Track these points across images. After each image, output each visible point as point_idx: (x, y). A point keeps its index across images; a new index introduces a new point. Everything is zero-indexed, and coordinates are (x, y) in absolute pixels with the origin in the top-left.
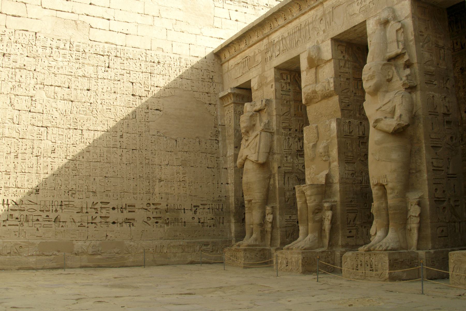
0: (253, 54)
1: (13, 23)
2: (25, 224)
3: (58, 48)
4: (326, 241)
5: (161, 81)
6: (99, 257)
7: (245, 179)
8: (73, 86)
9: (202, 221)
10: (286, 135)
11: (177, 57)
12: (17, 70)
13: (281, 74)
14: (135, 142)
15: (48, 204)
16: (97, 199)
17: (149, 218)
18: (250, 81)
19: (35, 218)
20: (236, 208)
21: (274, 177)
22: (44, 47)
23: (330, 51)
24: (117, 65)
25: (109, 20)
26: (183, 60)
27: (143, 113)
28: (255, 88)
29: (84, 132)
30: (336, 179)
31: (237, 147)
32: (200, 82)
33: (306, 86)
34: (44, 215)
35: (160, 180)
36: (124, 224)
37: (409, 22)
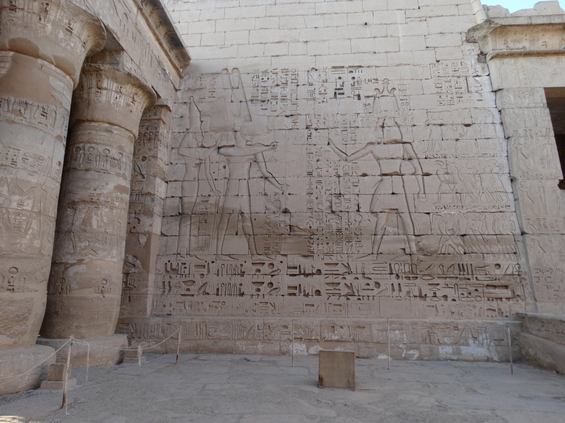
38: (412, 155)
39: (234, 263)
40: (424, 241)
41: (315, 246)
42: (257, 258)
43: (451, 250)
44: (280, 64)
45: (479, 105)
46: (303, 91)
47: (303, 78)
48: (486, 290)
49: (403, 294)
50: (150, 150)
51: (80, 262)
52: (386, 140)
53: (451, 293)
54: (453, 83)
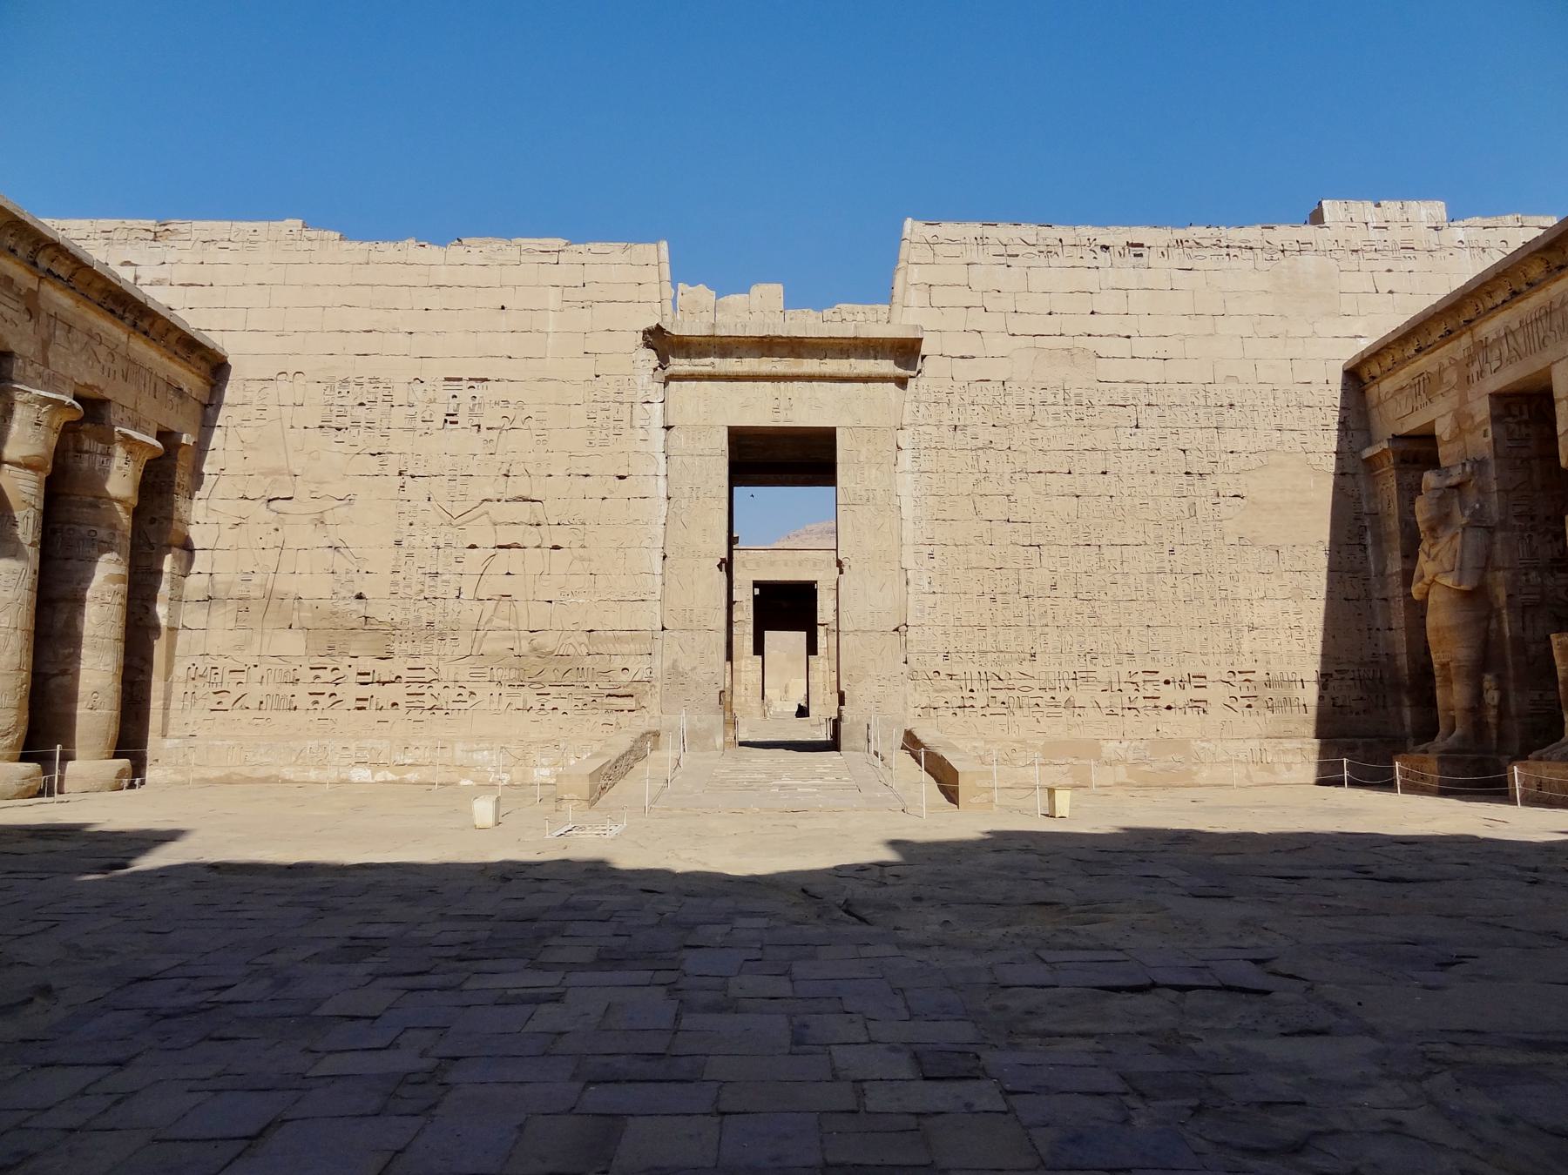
1: (963, 370)
2: (1018, 712)
3: (1043, 403)
6: (1146, 768)
7: (1431, 621)
8: (1076, 470)
9: (1340, 702)
12: (980, 452)
15: (1052, 676)
16: (1137, 666)
19: (1034, 701)
22: (1020, 405)
26: (1279, 394)
27: (1209, 505)
29: (1104, 550)
31: (1410, 555)
32: (1320, 433)
34: (1047, 696)
35: (1252, 628)
38: (542, 519)
39: (284, 668)
40: (539, 639)
41: (396, 645)
42: (317, 662)
43: (571, 651)
44: (366, 368)
45: (642, 447)
46: (398, 417)
47: (399, 396)
48: (606, 700)
49: (503, 706)
50: (161, 508)
51: (64, 672)
52: (510, 495)
53: (563, 705)
54: (612, 413)
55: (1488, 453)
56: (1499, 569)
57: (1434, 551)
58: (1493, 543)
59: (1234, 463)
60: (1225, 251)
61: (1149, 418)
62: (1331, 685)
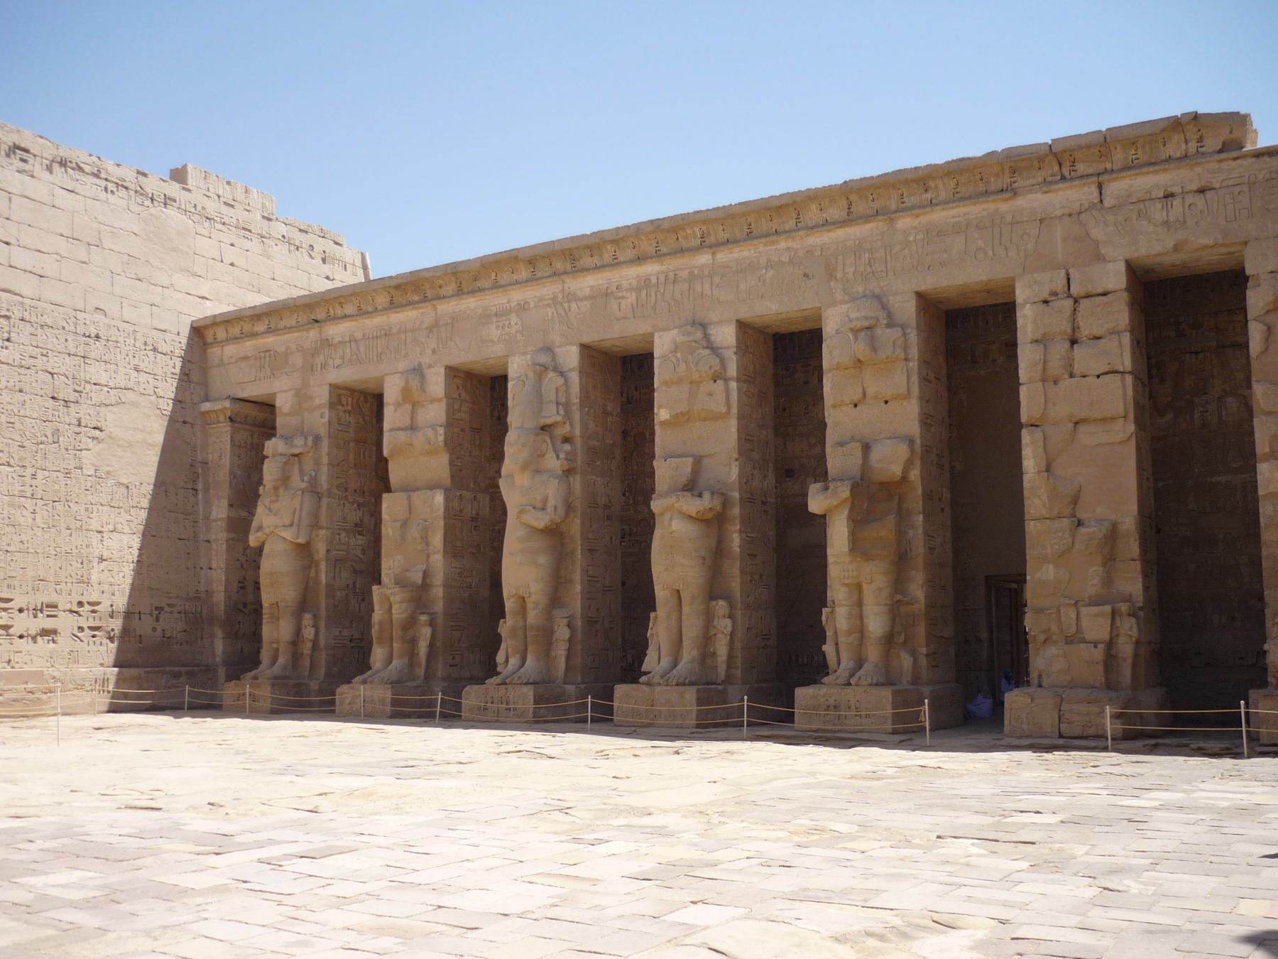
0: (283, 349)
4: (421, 672)
5: (104, 374)
10: (340, 499)
11: (131, 328)
13: (339, 396)
14: (57, 487)
17: (81, 629)
18: (275, 394)
20: (226, 612)
21: (317, 565)
23: (443, 385)
24: (24, 338)
25: (7, 243)
26: (139, 336)
28: (286, 409)
30: (438, 579)
33: (391, 430)
35: (102, 559)
36: (39, 638)
37: (575, 378)
55: (323, 431)
56: (321, 528)
57: (274, 507)
58: (320, 507)
59: (97, 396)
60: (103, 183)
61: (22, 334)
62: (162, 617)
